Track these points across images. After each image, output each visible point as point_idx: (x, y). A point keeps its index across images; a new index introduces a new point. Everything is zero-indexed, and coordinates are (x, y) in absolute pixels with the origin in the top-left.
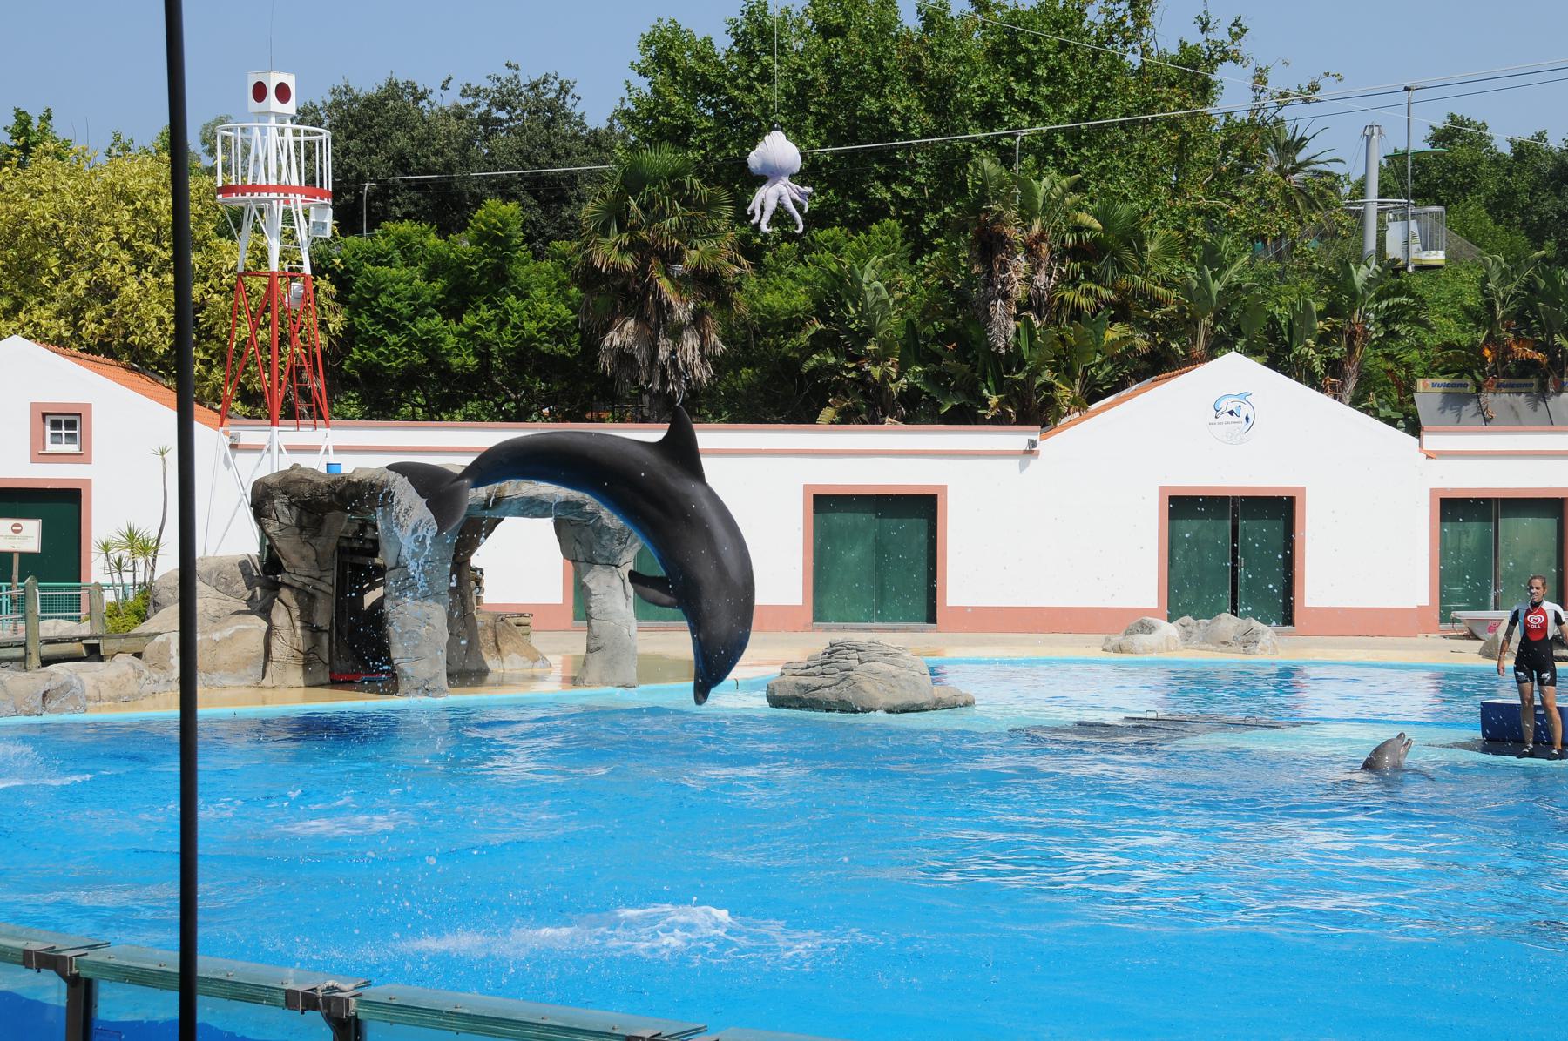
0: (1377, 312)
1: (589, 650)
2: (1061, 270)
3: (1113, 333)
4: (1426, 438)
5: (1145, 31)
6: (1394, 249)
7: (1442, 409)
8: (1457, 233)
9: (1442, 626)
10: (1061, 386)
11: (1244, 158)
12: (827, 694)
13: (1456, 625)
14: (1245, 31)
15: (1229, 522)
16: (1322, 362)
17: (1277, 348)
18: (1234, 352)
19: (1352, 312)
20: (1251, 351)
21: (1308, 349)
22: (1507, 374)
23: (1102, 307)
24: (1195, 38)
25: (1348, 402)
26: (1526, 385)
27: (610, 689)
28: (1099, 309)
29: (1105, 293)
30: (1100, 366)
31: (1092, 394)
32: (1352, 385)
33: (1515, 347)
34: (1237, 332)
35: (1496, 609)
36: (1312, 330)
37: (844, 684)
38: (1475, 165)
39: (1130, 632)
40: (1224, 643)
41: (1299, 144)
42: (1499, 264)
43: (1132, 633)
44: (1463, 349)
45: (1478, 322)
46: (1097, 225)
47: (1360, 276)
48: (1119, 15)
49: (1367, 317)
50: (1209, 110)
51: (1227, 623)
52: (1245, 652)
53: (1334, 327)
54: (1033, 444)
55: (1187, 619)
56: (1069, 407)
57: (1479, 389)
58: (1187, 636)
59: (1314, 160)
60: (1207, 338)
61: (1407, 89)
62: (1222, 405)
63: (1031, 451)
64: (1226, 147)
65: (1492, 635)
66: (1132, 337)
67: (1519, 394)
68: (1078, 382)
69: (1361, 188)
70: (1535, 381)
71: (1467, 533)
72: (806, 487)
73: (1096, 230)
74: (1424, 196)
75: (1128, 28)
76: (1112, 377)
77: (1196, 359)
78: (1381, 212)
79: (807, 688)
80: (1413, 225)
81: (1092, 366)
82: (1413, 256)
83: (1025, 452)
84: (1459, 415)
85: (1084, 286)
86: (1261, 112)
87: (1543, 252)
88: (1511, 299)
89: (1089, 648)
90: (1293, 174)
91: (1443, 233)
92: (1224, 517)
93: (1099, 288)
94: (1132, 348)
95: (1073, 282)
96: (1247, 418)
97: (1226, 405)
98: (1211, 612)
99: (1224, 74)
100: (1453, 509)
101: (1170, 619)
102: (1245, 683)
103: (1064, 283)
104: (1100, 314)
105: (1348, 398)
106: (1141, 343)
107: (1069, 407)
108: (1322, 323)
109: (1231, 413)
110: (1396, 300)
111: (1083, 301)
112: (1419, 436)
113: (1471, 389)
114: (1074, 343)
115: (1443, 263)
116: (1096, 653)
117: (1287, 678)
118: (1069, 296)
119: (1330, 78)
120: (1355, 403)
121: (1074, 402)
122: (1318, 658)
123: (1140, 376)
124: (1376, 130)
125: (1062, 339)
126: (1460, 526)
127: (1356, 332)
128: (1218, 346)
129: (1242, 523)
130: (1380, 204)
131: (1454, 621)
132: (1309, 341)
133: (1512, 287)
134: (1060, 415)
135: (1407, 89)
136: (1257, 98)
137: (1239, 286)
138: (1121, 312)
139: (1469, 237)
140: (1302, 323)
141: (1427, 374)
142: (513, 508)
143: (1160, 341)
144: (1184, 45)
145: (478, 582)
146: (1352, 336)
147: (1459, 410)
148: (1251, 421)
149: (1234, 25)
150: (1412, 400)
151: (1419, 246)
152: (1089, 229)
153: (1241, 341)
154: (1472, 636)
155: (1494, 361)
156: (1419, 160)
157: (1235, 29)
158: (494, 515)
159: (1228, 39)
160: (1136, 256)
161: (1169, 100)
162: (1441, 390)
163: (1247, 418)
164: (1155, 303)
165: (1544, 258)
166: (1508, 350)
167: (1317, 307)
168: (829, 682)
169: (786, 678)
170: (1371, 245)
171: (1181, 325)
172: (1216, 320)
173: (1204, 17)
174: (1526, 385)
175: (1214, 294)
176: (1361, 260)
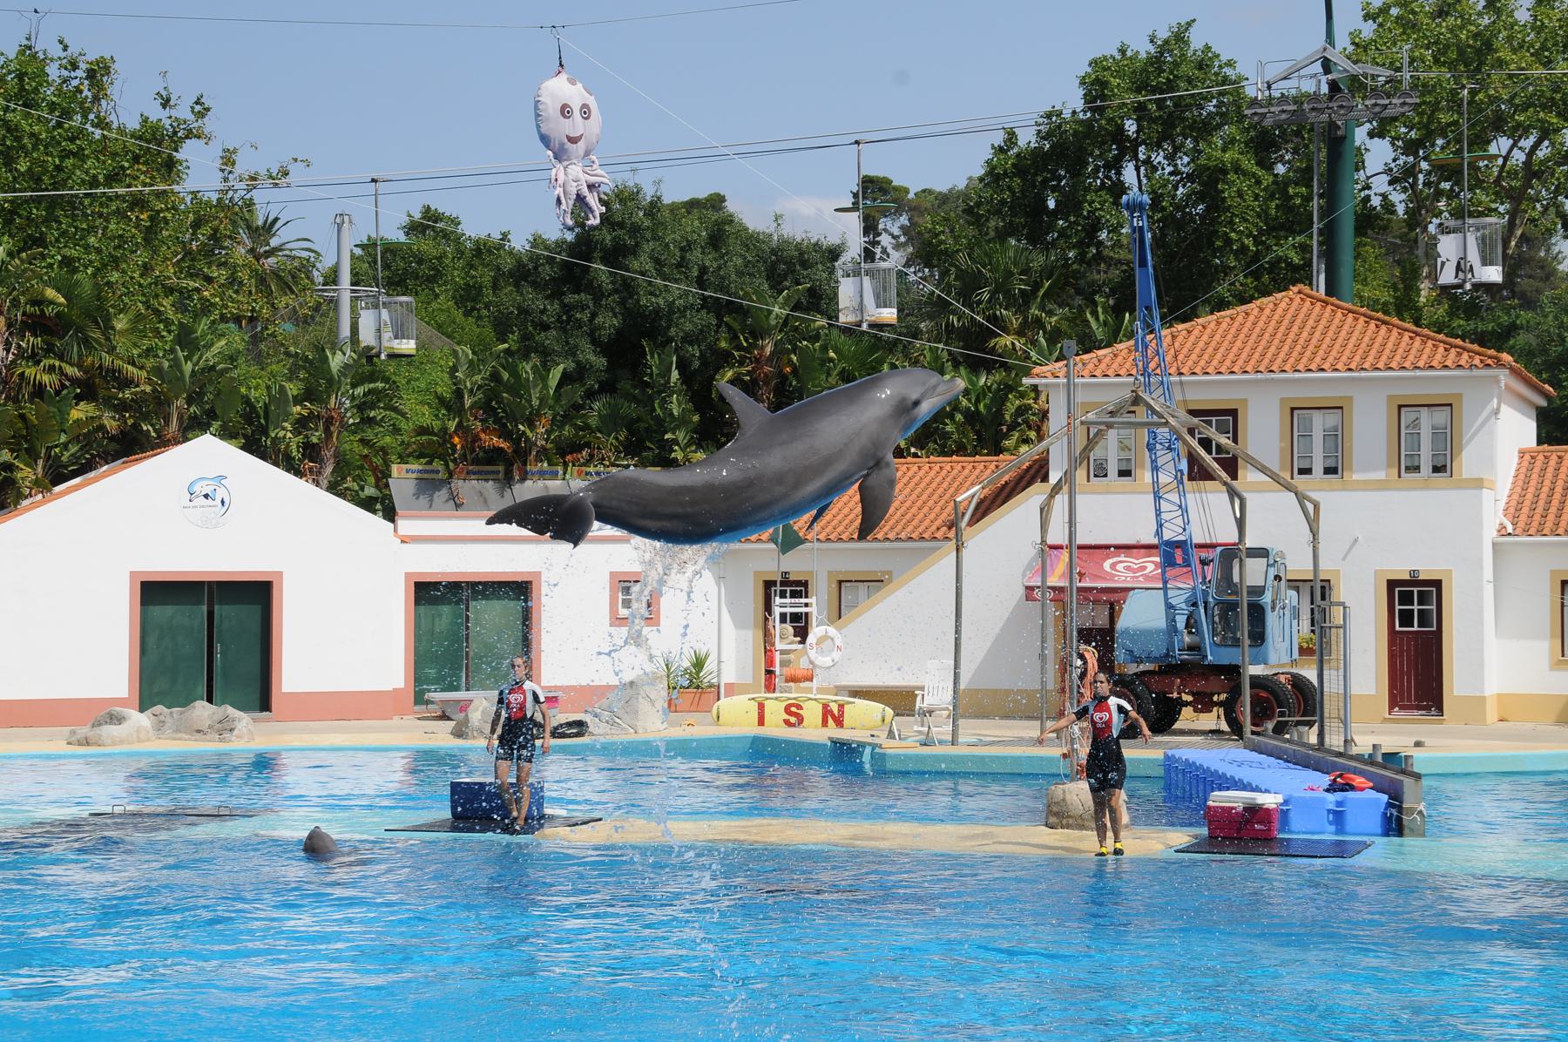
0: (353, 398)
2: (19, 346)
3: (80, 412)
4: (400, 522)
5: (103, 102)
6: (367, 337)
7: (417, 495)
8: (428, 323)
9: (417, 708)
10: (22, 466)
11: (215, 236)
13: (430, 706)
14: (208, 110)
15: (205, 608)
16: (298, 447)
17: (253, 431)
18: (208, 435)
19: (329, 397)
20: (227, 434)
21: (285, 432)
22: (476, 461)
23: (67, 383)
24: (156, 113)
25: (325, 486)
26: (493, 472)
28: (63, 386)
29: (71, 370)
30: (65, 446)
31: (57, 475)
32: (329, 469)
33: (483, 436)
34: (212, 415)
35: (468, 690)
36: (289, 414)
38: (439, 258)
39: (98, 724)
40: (199, 731)
41: (269, 227)
42: (467, 355)
43: (100, 725)
44: (435, 435)
45: (449, 409)
46: (62, 300)
47: (336, 361)
48: (75, 83)
49: (342, 402)
50: (176, 188)
51: (202, 711)
53: (312, 412)
55: (159, 708)
56: (31, 489)
57: (451, 475)
58: (159, 726)
59: (288, 246)
60: (180, 418)
61: (374, 181)
62: (197, 488)
64: (196, 225)
65: (463, 715)
66: (100, 417)
67: (487, 480)
68: (40, 462)
69: (332, 278)
70: (501, 468)
71: (440, 616)
73: (60, 305)
74: (398, 284)
75: (87, 97)
76: (79, 458)
77: (169, 440)
78: (354, 300)
80: (385, 314)
81: (56, 446)
82: (385, 344)
84: (431, 501)
85: (46, 362)
86: (231, 193)
87: (506, 345)
88: (478, 389)
89: (52, 741)
90: (267, 258)
91: (413, 323)
92: (199, 603)
93: (63, 365)
94: (102, 428)
95: (34, 358)
96: (223, 502)
98: (186, 701)
99: (189, 152)
100: (426, 592)
101: (142, 710)
102: (220, 769)
103: (23, 358)
104: (65, 392)
105: (325, 483)
106: (110, 422)
107: (31, 489)
108: (299, 408)
109: (206, 496)
110: (372, 385)
111: (46, 378)
112: (392, 520)
113: (442, 475)
114: (36, 422)
115: (414, 352)
116: (60, 747)
117: (264, 764)
118: (30, 372)
119: (299, 163)
120: (333, 488)
121: (37, 483)
122: (296, 744)
123: (115, 457)
124: (346, 218)
125: (22, 417)
126: (433, 609)
127: (333, 418)
128: (193, 427)
129: (216, 607)
130: (353, 291)
131: (428, 702)
132: (286, 424)
133: (478, 378)
134: (20, 496)
135: (374, 181)
136: (226, 180)
137: (213, 368)
138: (87, 391)
139: (439, 327)
140: (278, 407)
141: (403, 459)
143: (130, 422)
144: (146, 120)
146: (329, 421)
147: (432, 496)
148: (227, 504)
149: (196, 103)
150: (387, 486)
151: (391, 334)
152: (52, 302)
153: (216, 425)
154: (444, 717)
155: (463, 447)
156: (391, 249)
157: (198, 108)
159: (192, 117)
160: (104, 334)
161: (136, 178)
162: (414, 475)
163: (223, 502)
164: (127, 382)
165: (508, 352)
166: (476, 438)
167: (293, 389)
170: (345, 331)
171: (158, 404)
172: (190, 402)
173: (164, 94)
174: (493, 472)
175: (187, 376)
176: (335, 346)
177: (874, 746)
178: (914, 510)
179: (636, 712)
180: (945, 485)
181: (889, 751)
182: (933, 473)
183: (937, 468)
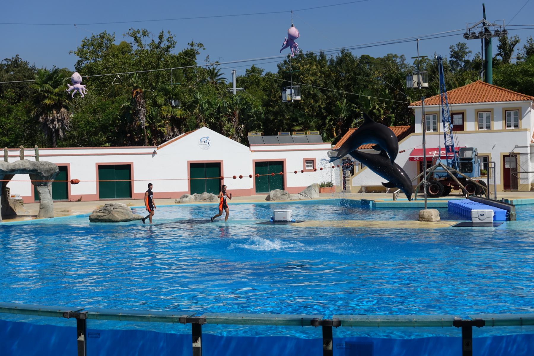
1: (40, 208)
4: (251, 147)
12: (105, 218)
27: (46, 219)
37: (110, 215)
51: (206, 195)
54: (154, 151)
55: (196, 194)
58: (196, 199)
62: (202, 140)
63: (154, 153)
72: (96, 163)
79: (99, 216)
83: (153, 153)
97: (203, 140)
100: (259, 165)
101: (191, 194)
109: (204, 142)
112: (249, 147)
142: (18, 172)
145: (9, 191)
158: (13, 174)
168: (106, 214)
179: (311, 194)
181: (376, 202)
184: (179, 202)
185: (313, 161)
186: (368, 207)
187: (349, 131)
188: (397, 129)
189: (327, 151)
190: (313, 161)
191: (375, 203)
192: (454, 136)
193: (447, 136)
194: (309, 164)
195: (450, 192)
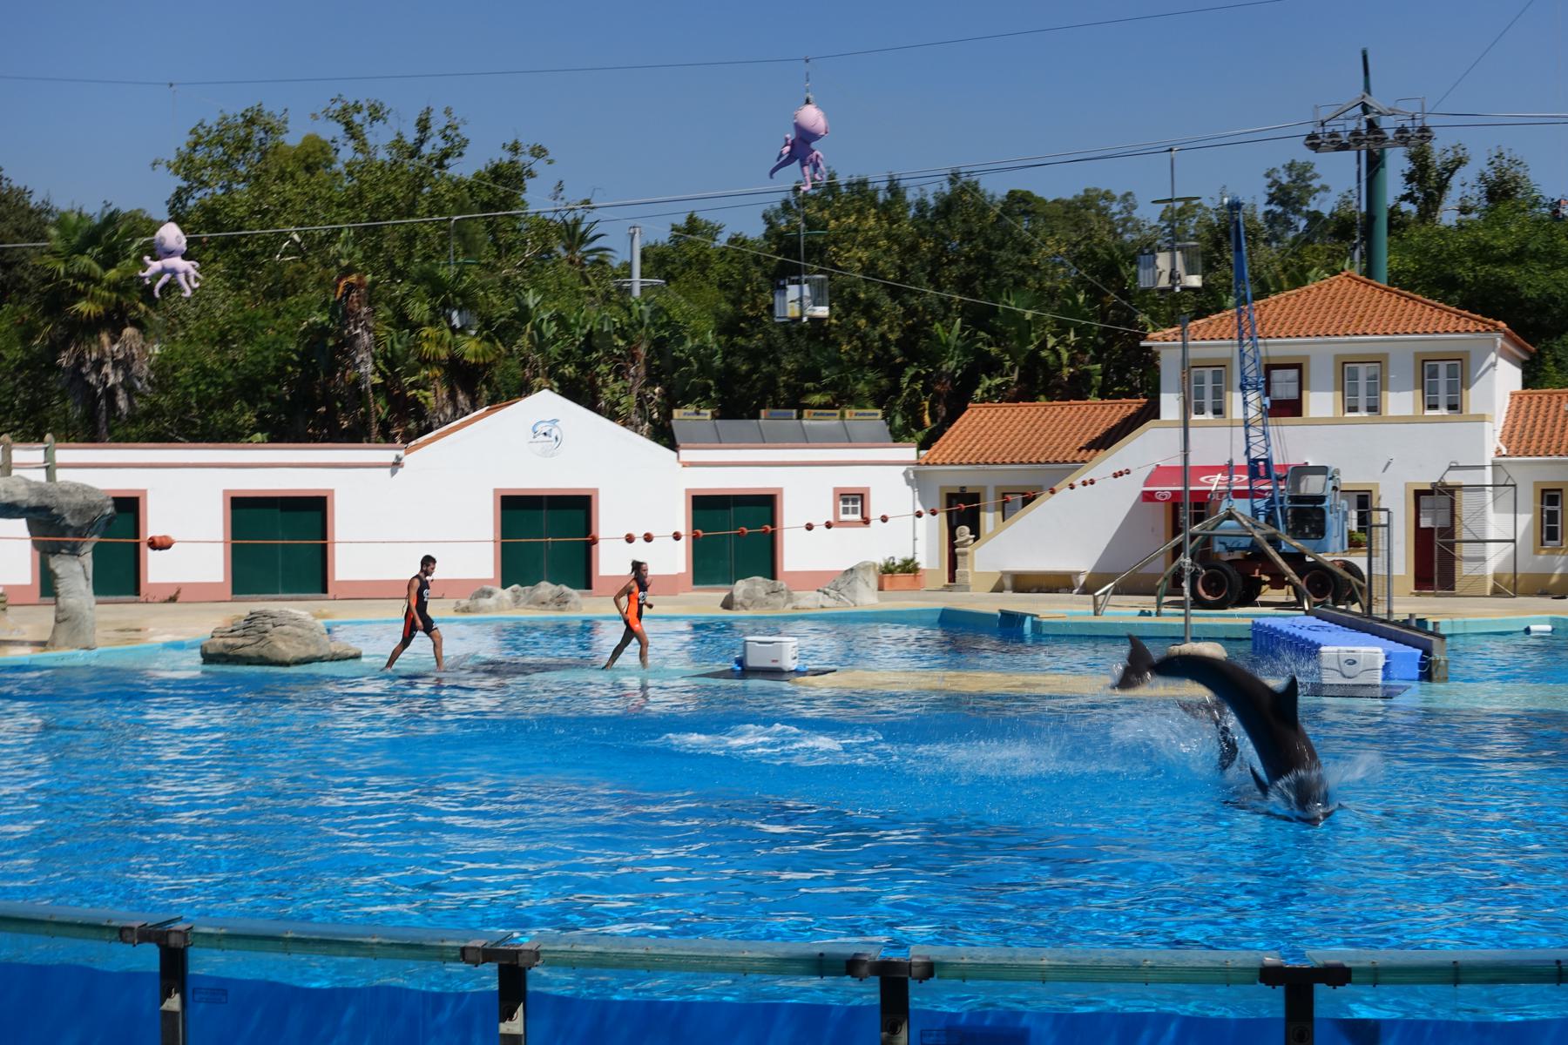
1: (57, 621)
4: (682, 452)
12: (250, 651)
27: (74, 651)
37: (262, 643)
51: (546, 589)
52: (561, 610)
54: (397, 457)
55: (516, 586)
58: (516, 600)
62: (538, 428)
63: (397, 464)
79: (232, 647)
83: (394, 464)
97: (542, 428)
100: (705, 506)
101: (504, 586)
112: (676, 451)
168: (250, 642)
169: (215, 640)
177: (1033, 616)
178: (1059, 440)
179: (855, 591)
180: (1082, 421)
182: (1072, 413)
183: (1075, 408)
184: (467, 610)
185: (862, 495)
186: (1021, 638)
187: (968, 411)
188: (1108, 407)
189: (904, 468)
190: (862, 495)
191: (1040, 623)
192: (1272, 430)
193: (1252, 432)
194: (850, 505)
195: (1258, 593)
